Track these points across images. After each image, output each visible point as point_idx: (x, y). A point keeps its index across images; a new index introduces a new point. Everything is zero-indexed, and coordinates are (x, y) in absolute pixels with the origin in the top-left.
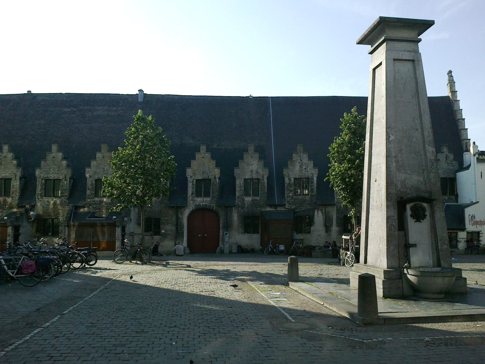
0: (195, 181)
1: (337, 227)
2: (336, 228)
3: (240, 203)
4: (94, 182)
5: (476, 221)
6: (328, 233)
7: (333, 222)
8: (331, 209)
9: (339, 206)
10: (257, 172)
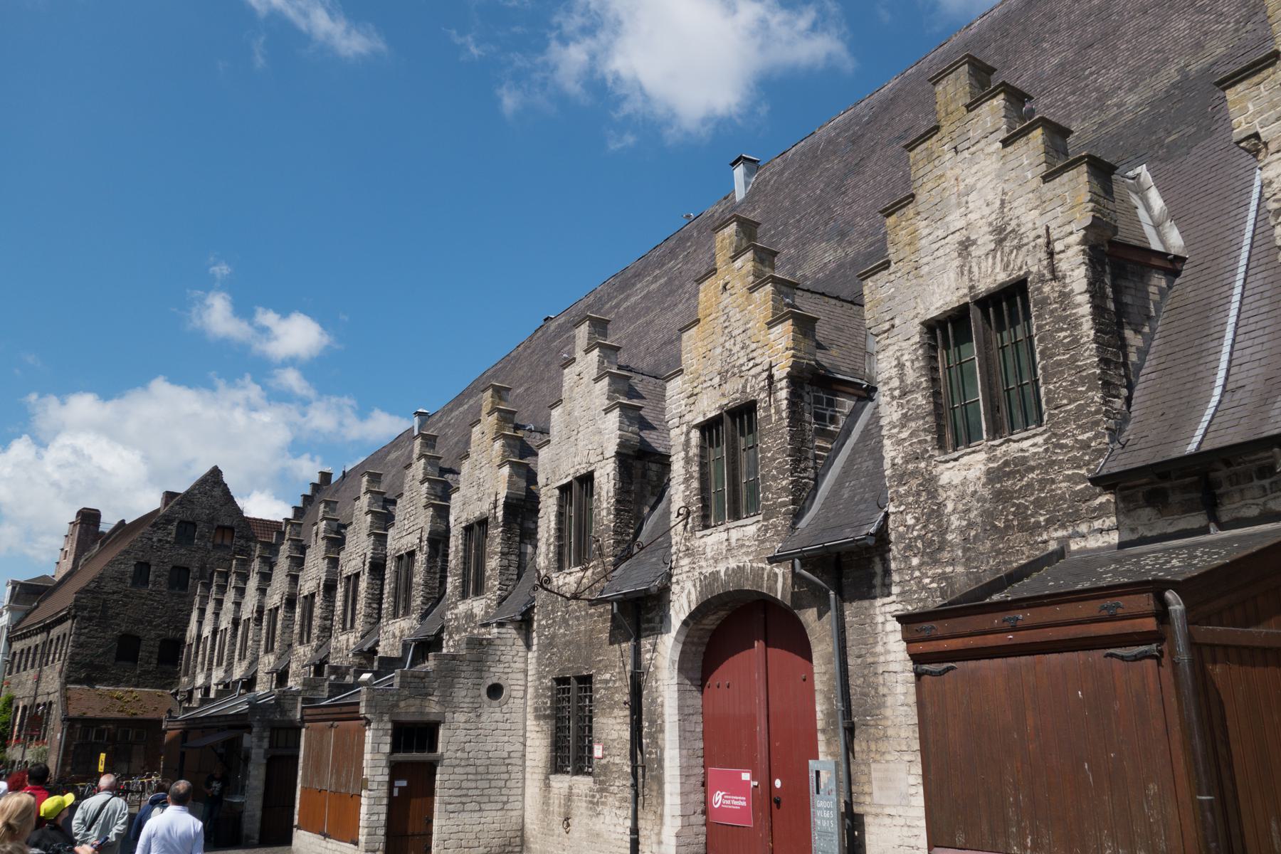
0: (695, 435)
3: (910, 521)
4: (460, 541)
10: (1001, 234)
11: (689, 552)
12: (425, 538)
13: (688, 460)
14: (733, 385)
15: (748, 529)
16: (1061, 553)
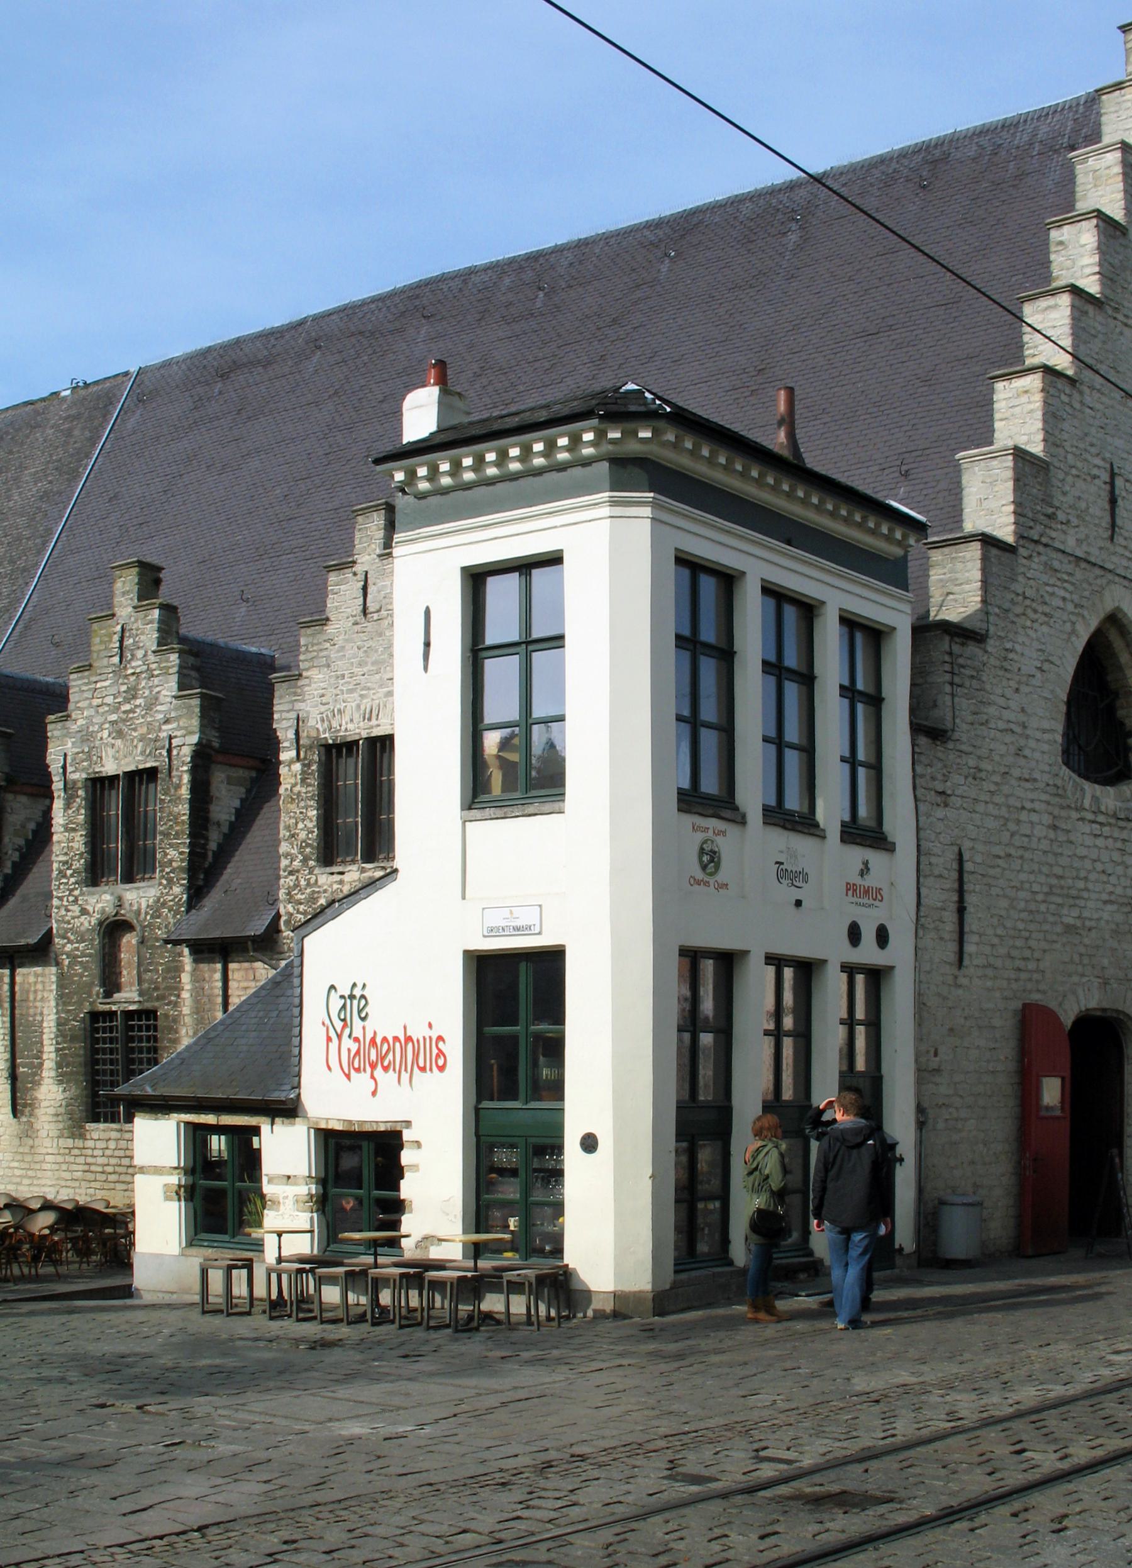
1: (60, 1082)
2: (54, 1088)
5: (373, 1041)
6: (24, 1119)
7: (42, 1052)
8: (37, 975)
9: (68, 955)
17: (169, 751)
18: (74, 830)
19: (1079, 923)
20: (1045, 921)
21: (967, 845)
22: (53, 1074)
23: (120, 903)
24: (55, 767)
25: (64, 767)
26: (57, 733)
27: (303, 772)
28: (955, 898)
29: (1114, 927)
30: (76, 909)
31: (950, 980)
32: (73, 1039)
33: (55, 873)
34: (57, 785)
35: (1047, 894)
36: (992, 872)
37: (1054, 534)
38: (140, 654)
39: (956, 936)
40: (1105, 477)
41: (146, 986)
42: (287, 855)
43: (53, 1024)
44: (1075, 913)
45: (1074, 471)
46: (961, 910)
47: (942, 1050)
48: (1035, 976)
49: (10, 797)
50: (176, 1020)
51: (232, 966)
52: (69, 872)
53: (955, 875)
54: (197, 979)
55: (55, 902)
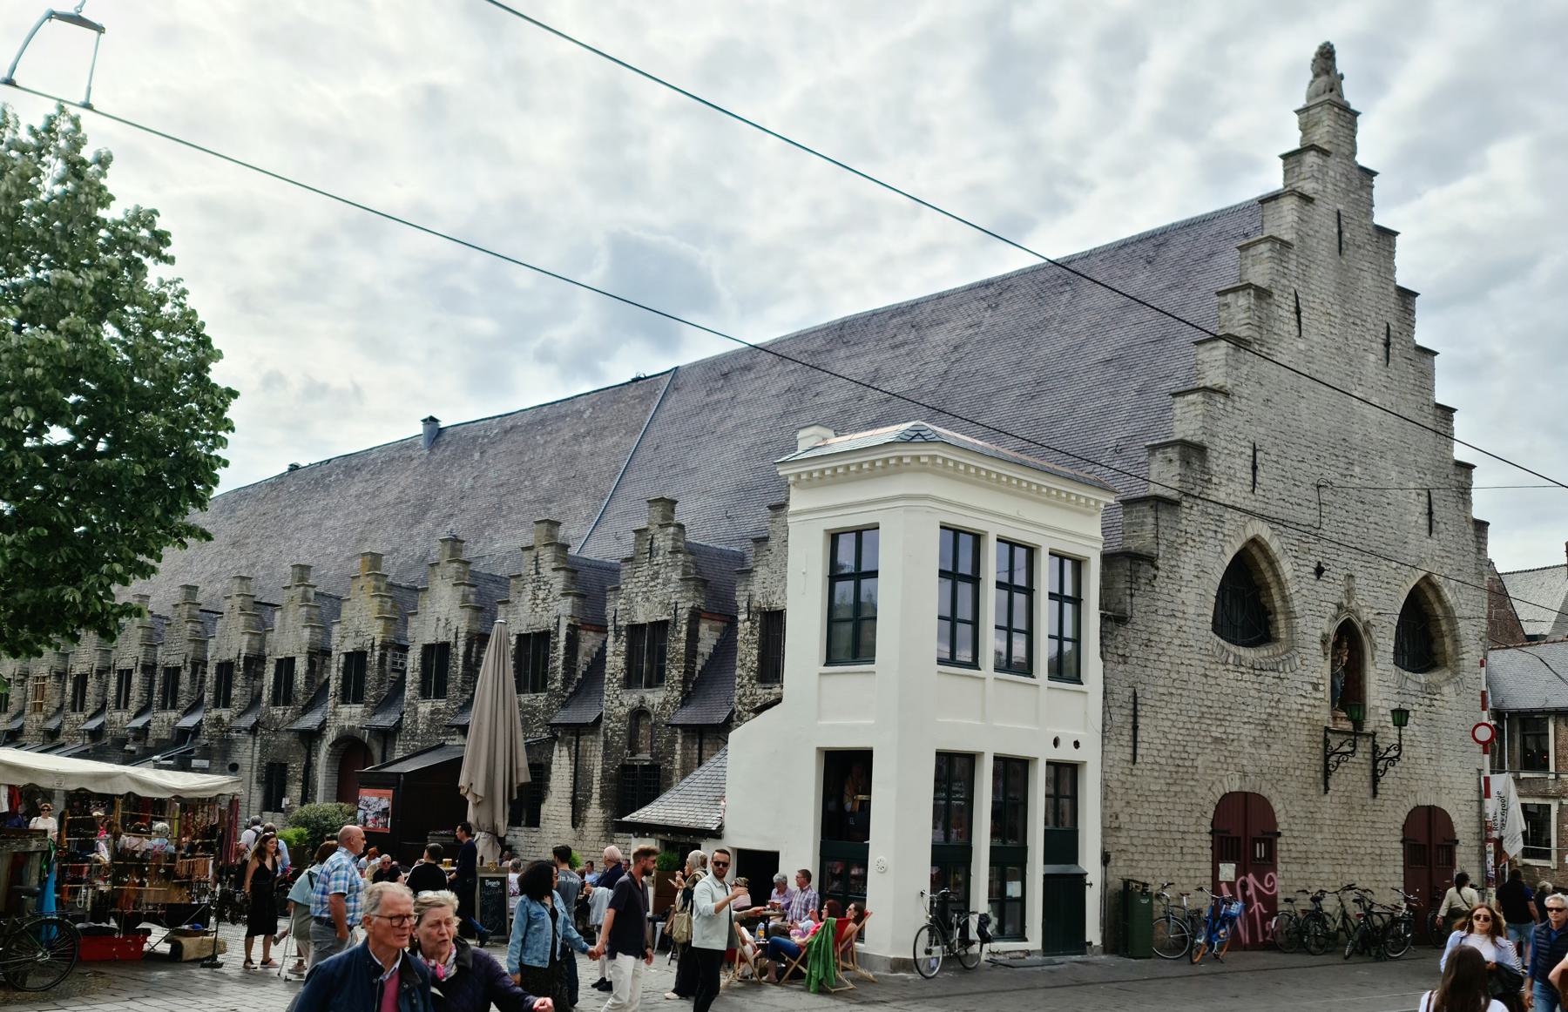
0: (342, 658)
2: (598, 811)
6: (579, 829)
9: (611, 730)
11: (335, 714)
12: (189, 660)
13: (338, 670)
14: (360, 640)
15: (357, 709)
16: (443, 745)
17: (675, 611)
18: (618, 655)
19: (1224, 736)
20: (1198, 735)
21: (1140, 687)
22: (598, 802)
23: (642, 700)
24: (610, 618)
25: (615, 617)
26: (612, 597)
27: (751, 627)
28: (1131, 720)
29: (1252, 739)
30: (617, 703)
31: (1127, 771)
32: (611, 781)
33: (606, 681)
34: (611, 627)
35: (1200, 718)
36: (1158, 704)
37: (1209, 492)
38: (661, 552)
39: (1131, 744)
40: (1250, 452)
41: (654, 751)
42: (740, 676)
43: (599, 771)
44: (1222, 729)
45: (1226, 451)
46: (1135, 728)
47: (1121, 816)
48: (1190, 770)
49: (584, 632)
50: (671, 772)
51: (705, 741)
52: (614, 680)
53: (1131, 706)
54: (684, 748)
55: (606, 698)
